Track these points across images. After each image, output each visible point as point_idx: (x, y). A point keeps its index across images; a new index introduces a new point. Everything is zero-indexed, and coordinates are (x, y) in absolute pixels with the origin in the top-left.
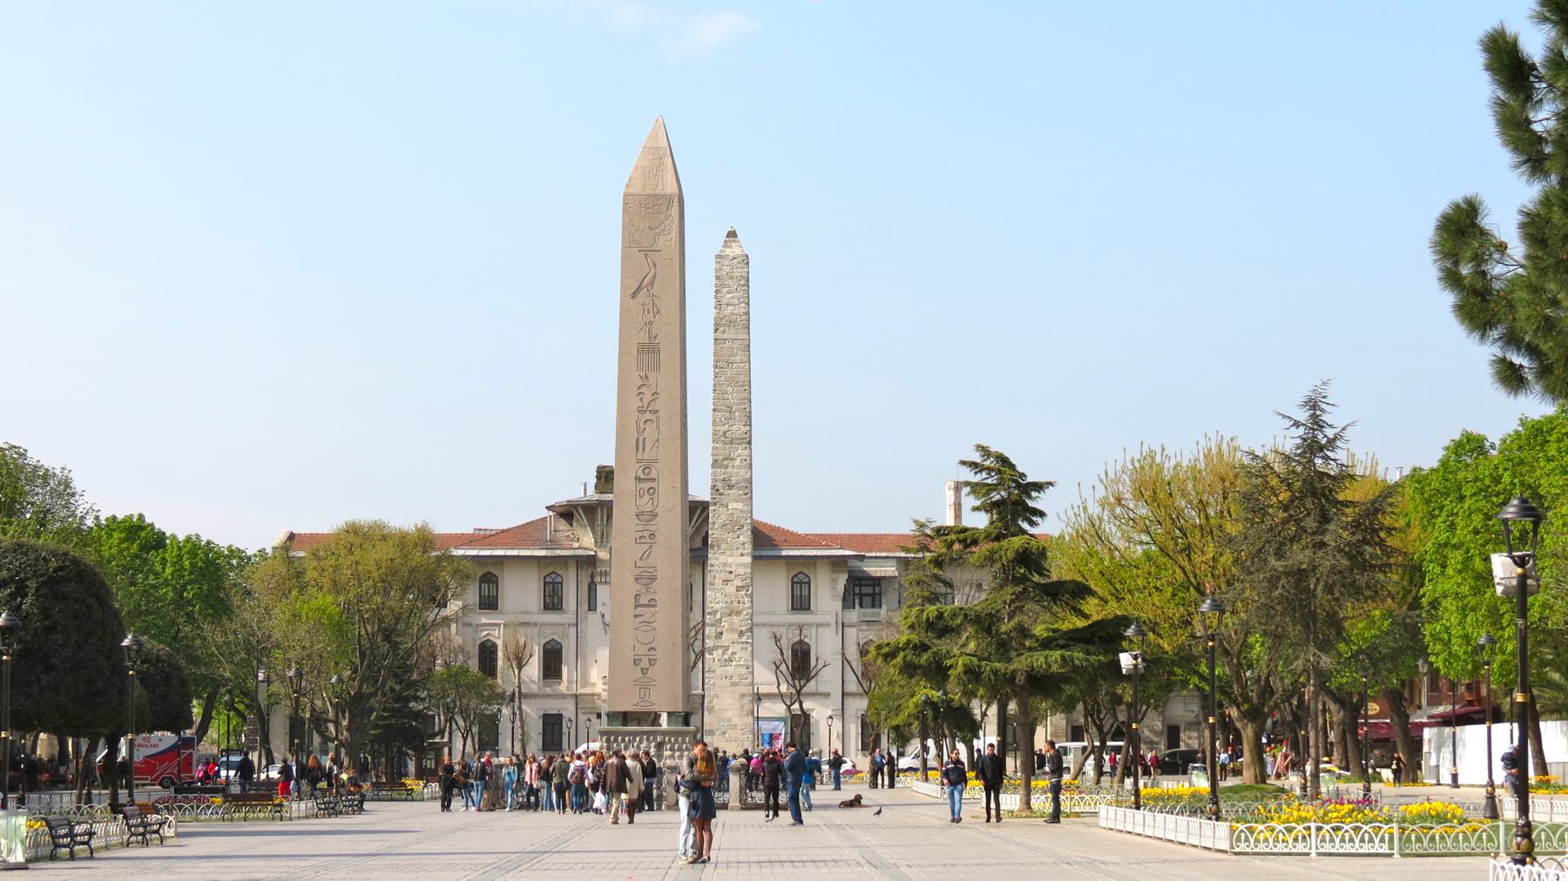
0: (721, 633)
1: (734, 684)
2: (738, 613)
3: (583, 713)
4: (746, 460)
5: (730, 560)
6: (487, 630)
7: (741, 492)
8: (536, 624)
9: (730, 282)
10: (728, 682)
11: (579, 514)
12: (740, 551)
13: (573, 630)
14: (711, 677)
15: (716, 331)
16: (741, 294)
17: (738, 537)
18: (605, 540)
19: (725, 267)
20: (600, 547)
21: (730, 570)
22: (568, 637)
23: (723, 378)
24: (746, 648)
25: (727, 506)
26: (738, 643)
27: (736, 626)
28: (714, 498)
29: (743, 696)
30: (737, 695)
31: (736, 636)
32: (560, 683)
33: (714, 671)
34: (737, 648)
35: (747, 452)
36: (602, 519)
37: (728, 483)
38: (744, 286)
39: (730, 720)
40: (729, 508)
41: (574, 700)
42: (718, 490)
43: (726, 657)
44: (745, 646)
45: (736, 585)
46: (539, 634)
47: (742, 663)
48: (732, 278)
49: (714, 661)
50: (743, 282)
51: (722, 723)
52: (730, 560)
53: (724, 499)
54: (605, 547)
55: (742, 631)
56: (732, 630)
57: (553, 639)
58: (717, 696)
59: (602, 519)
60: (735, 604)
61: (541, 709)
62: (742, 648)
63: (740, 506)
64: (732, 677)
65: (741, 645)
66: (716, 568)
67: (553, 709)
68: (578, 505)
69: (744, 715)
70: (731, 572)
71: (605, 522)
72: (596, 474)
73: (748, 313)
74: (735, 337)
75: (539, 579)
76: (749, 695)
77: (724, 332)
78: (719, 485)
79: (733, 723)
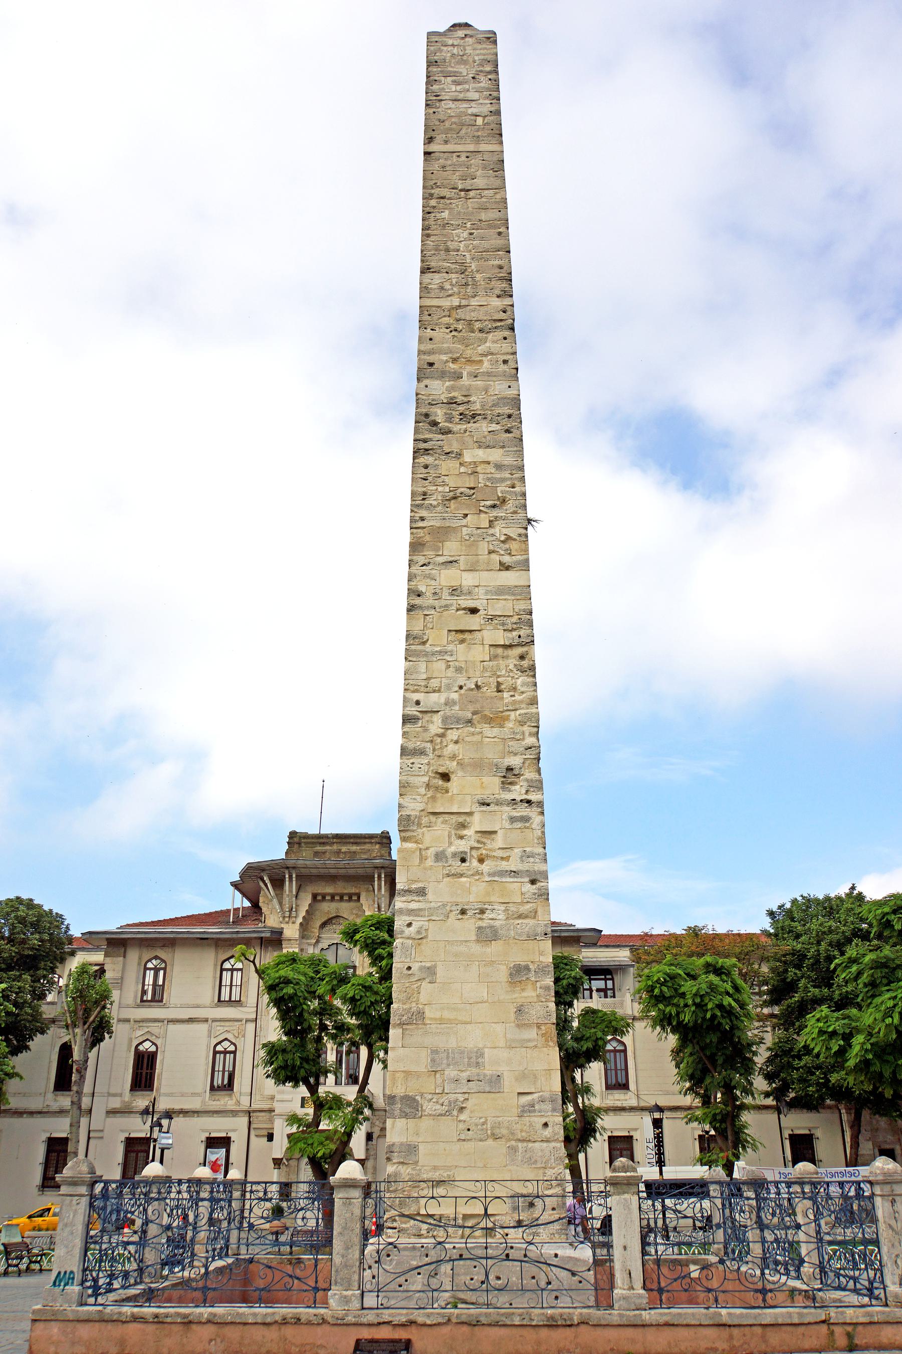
0: (445, 777)
1: (488, 935)
2: (497, 720)
3: (256, 1136)
4: (505, 362)
5: (468, 580)
6: (148, 1027)
7: (494, 427)
8: (206, 1020)
9: (462, 69)
10: (470, 925)
11: (266, 885)
12: (495, 558)
13: (251, 1027)
14: (410, 912)
15: (429, 140)
16: (482, 85)
17: (491, 523)
18: (294, 914)
19: (450, 48)
20: (287, 923)
21: (471, 604)
22: (244, 1036)
23: (446, 214)
24: (526, 819)
25: (459, 455)
26: (498, 803)
27: (491, 754)
28: (425, 441)
29: (518, 973)
30: (503, 974)
31: (492, 785)
32: (230, 1095)
33: (422, 892)
34: (499, 819)
35: (506, 347)
36: (291, 891)
37: (461, 408)
38: (489, 73)
39: (476, 1058)
40: (468, 457)
41: (246, 1119)
42: (435, 424)
43: (462, 846)
44: (523, 811)
45: (488, 641)
46: (210, 1031)
47: (513, 864)
48: (465, 63)
49: (422, 859)
50: (488, 68)
51: (451, 1073)
52: (468, 580)
53: (451, 443)
54: (294, 923)
55: (509, 769)
56: (478, 766)
57: (226, 1039)
58: (431, 971)
59: (291, 891)
60: (489, 691)
61: (203, 1131)
62: (513, 820)
63: (495, 455)
64: (482, 912)
65: (507, 810)
66: (431, 602)
67: (220, 1131)
68: (263, 870)
69: (523, 1044)
70: (474, 611)
71: (294, 893)
72: (287, 840)
73: (498, 113)
74: (471, 148)
75: (216, 965)
76: (541, 970)
77: (446, 142)
78: (439, 414)
79: (488, 1071)
